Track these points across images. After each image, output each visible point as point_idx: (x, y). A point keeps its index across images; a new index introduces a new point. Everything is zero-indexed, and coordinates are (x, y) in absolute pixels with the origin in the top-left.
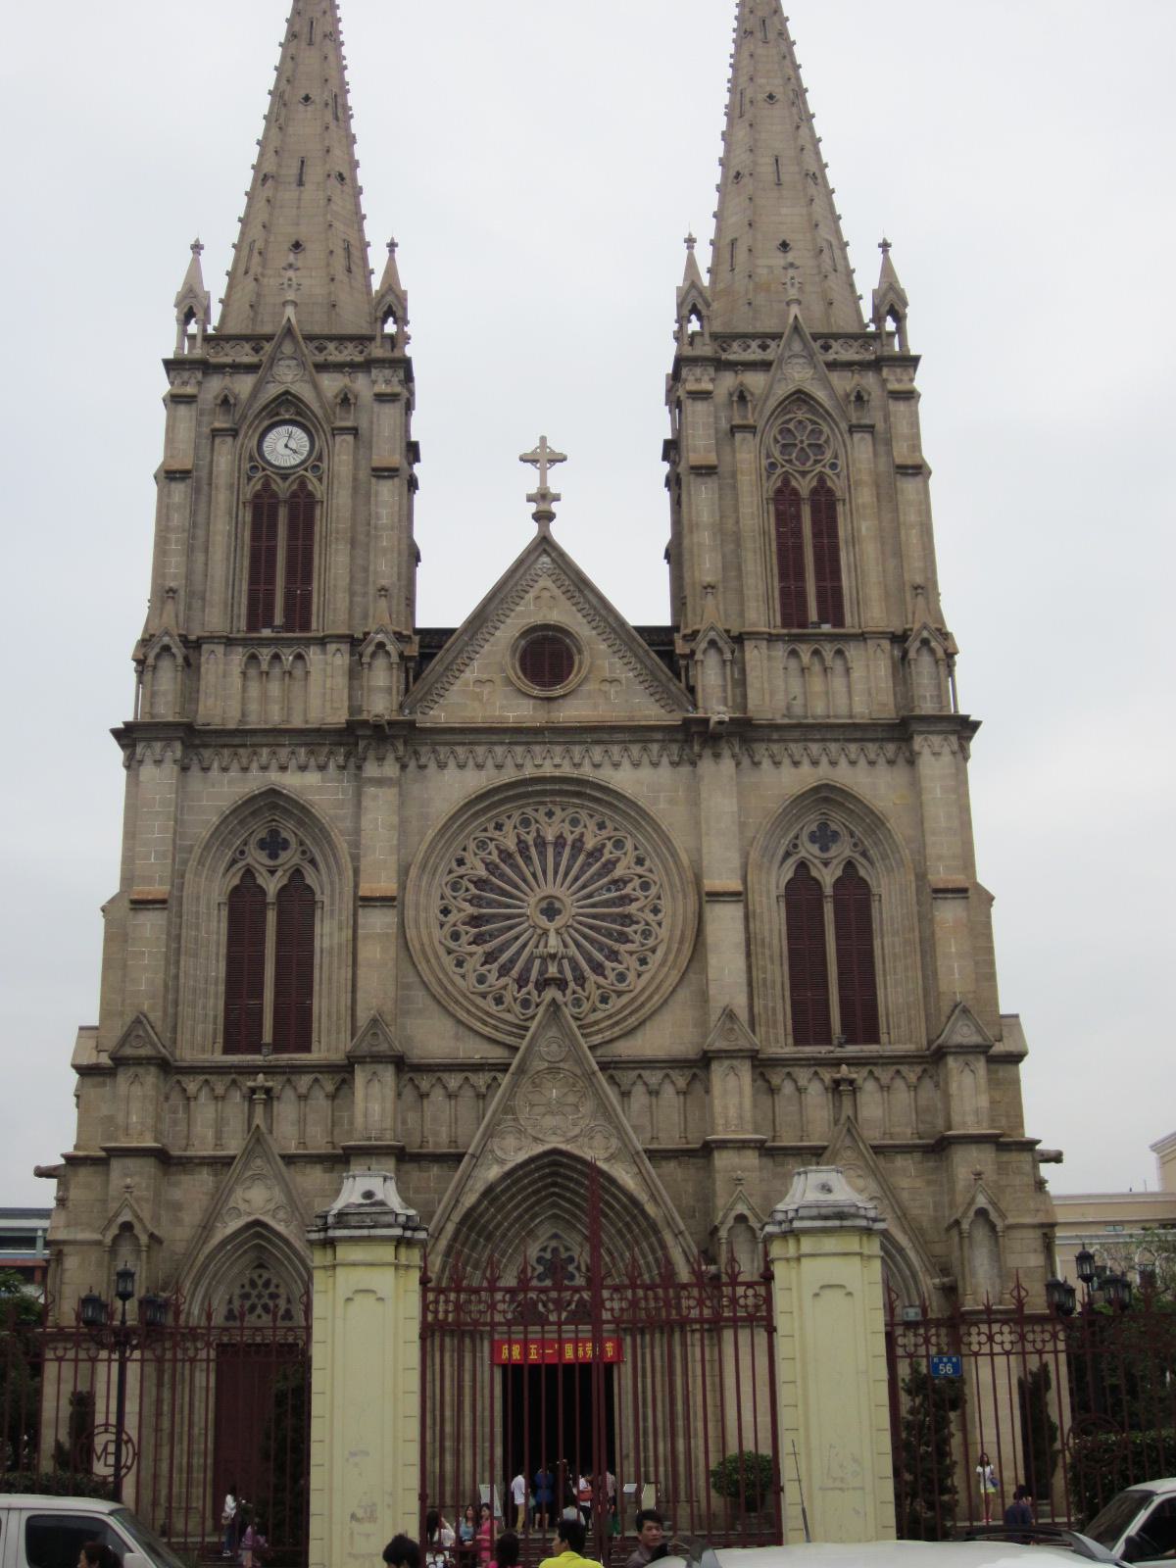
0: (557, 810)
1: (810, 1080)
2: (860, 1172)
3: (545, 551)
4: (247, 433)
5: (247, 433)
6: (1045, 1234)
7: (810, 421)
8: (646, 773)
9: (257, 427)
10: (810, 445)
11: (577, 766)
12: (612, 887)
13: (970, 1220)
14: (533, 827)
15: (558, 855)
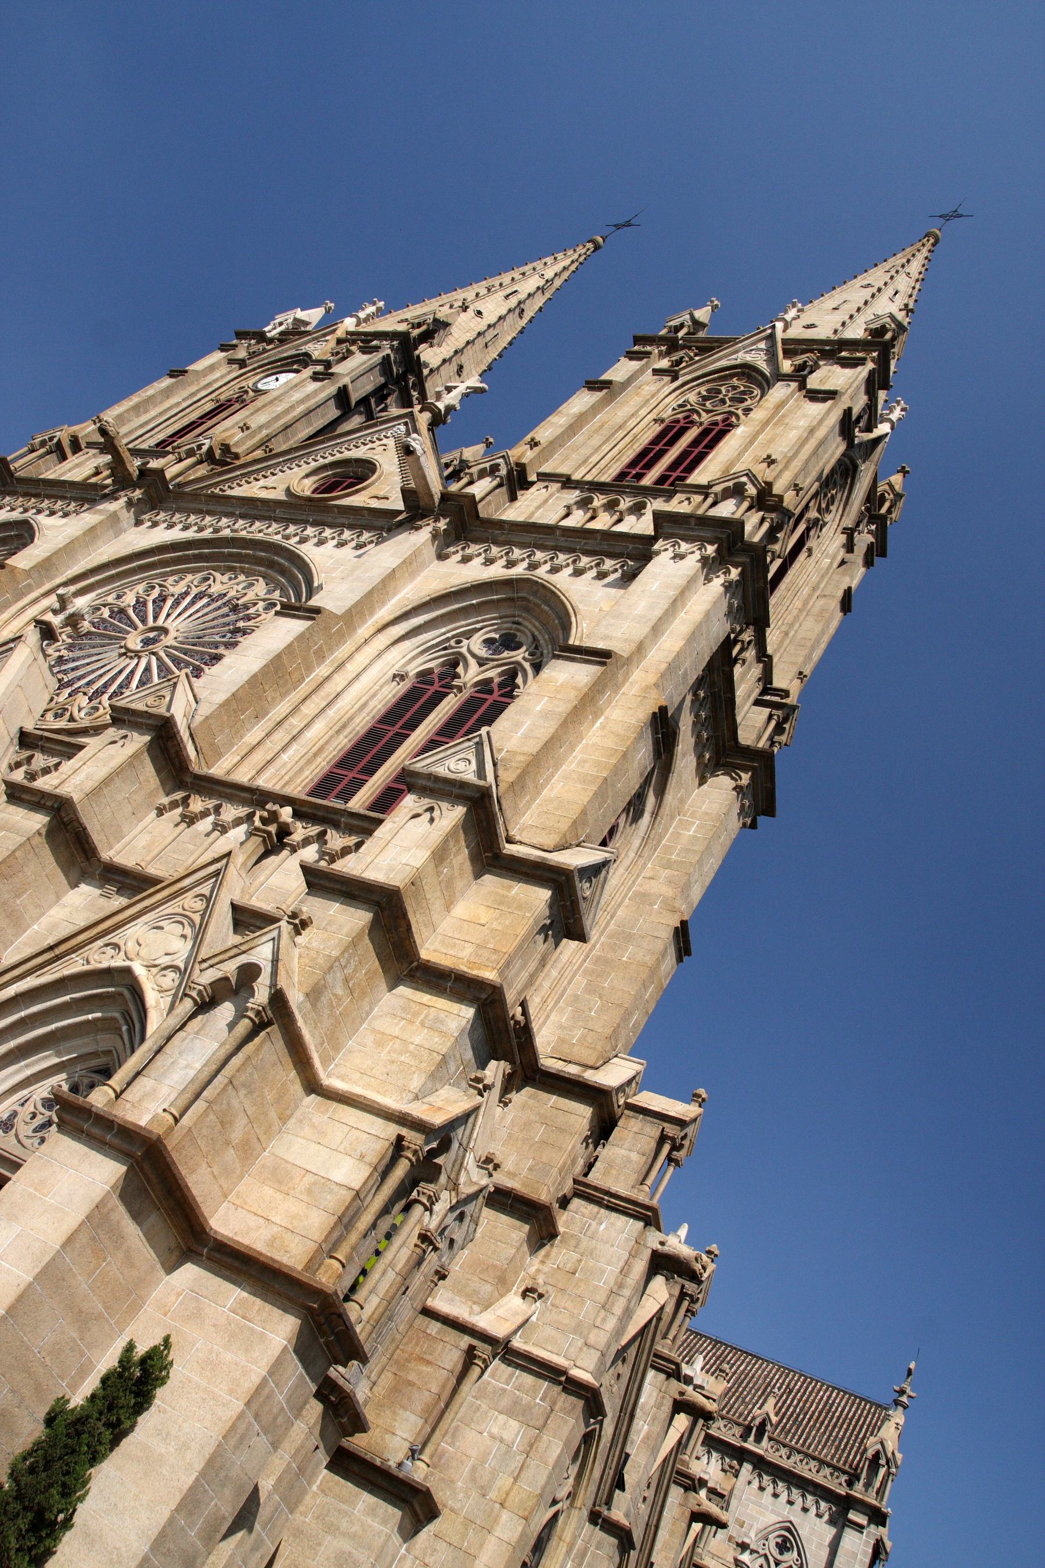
0: (242, 577)
1: (238, 822)
2: (188, 931)
3: (406, 424)
4: (254, 369)
5: (254, 369)
6: (400, 1138)
7: (745, 386)
8: (348, 551)
9: (268, 369)
10: (731, 399)
11: (287, 537)
12: (229, 635)
13: (219, 975)
14: (208, 583)
15: (208, 604)
